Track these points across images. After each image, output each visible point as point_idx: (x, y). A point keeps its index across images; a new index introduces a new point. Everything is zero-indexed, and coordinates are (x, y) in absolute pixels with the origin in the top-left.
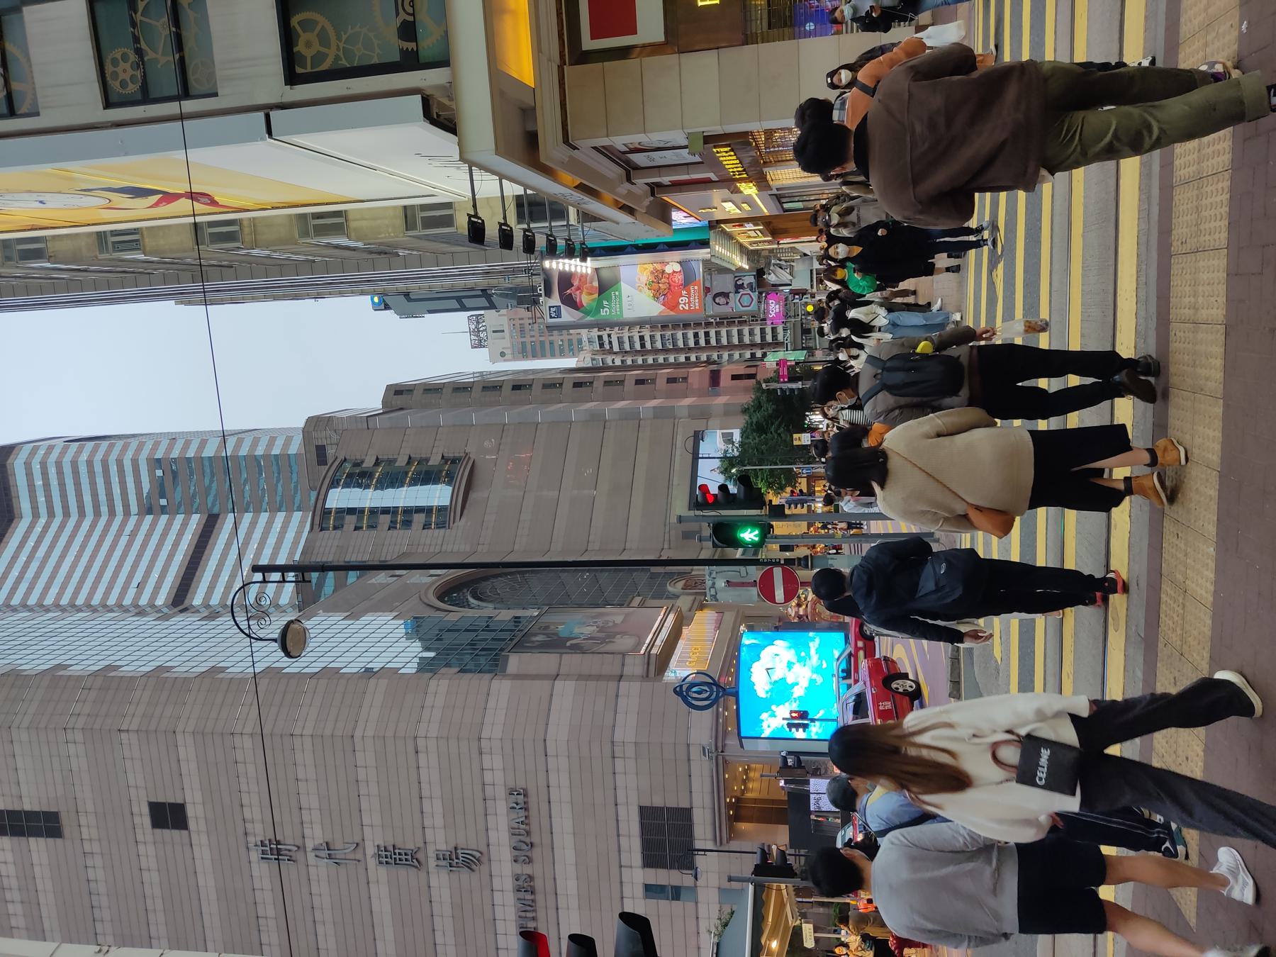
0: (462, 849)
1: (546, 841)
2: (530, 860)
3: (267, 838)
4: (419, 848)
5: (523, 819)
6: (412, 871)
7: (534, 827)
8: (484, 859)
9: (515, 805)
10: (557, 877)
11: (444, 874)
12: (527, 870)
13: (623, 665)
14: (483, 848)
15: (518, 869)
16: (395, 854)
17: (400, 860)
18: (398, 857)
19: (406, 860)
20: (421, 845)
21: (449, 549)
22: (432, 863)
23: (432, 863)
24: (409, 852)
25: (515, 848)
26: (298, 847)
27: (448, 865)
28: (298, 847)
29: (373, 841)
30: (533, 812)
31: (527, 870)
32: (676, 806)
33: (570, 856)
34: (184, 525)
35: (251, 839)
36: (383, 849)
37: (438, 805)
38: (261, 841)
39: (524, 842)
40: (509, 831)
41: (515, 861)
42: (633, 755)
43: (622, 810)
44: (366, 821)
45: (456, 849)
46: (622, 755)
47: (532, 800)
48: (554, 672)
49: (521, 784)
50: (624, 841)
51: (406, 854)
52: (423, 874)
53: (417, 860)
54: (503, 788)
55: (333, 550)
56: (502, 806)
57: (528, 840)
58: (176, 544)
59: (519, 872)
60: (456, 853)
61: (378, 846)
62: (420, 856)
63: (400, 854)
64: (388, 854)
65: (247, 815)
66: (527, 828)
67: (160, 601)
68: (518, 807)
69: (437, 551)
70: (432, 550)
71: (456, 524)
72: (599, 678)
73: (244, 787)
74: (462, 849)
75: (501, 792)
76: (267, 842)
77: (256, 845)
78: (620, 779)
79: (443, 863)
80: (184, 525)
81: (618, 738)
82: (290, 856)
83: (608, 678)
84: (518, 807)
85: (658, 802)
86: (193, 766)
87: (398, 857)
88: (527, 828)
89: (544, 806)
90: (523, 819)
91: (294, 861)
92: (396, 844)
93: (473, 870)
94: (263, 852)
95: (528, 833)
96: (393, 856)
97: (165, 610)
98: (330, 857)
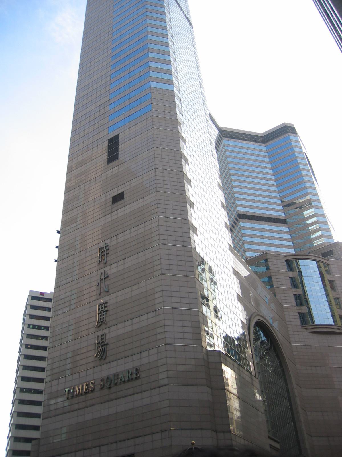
0: (107, 348)
2: (102, 388)
3: (110, 248)
4: (107, 324)
5: (123, 380)
9: (130, 373)
14: (107, 360)
16: (103, 312)
17: (101, 316)
18: (102, 314)
19: (101, 319)
22: (100, 333)
24: (104, 319)
25: (108, 378)
26: (106, 263)
27: (99, 342)
28: (106, 263)
29: (110, 300)
34: (278, 210)
35: (109, 241)
36: (106, 305)
37: (129, 329)
38: (108, 246)
40: (116, 373)
41: (101, 380)
44: (119, 293)
45: (107, 344)
49: (142, 375)
51: (103, 318)
53: (101, 325)
55: (275, 269)
56: (129, 366)
57: (112, 385)
58: (267, 209)
59: (97, 383)
61: (107, 303)
62: (103, 326)
63: (103, 315)
64: (104, 309)
65: (119, 236)
66: (118, 383)
67: (239, 209)
68: (129, 376)
69: (287, 323)
70: (287, 320)
71: (305, 330)
73: (132, 230)
75: (136, 364)
76: (107, 248)
77: (106, 244)
79: (100, 338)
80: (278, 210)
82: (101, 261)
86: (142, 204)
87: (102, 314)
90: (123, 380)
91: (99, 263)
92: (108, 312)
94: (103, 248)
95: (116, 384)
96: (102, 312)
97: (235, 212)
98: (101, 280)
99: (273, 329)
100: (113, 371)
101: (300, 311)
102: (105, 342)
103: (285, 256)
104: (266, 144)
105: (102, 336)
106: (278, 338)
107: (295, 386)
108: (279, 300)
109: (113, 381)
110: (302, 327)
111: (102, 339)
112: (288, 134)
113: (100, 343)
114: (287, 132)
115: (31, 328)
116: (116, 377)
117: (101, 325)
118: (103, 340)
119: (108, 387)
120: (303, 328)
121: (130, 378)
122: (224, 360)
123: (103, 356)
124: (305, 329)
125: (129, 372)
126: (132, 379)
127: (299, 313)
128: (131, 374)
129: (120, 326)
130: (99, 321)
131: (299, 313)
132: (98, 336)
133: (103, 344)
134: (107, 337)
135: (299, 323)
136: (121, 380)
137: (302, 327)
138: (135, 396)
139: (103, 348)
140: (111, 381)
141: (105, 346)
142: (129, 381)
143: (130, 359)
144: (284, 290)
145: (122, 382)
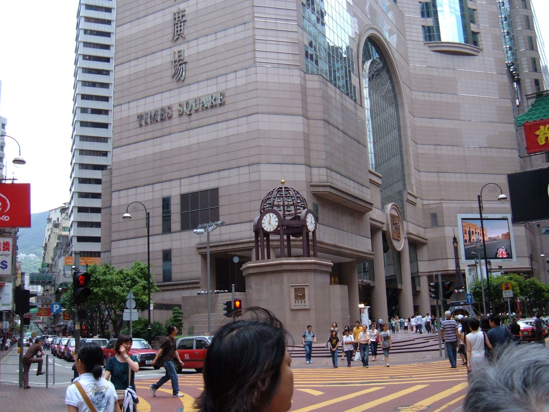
0: (185, 67)
1: (195, 124)
2: (181, 115)
4: (185, 38)
6: (171, 37)
7: (201, 114)
8: (180, 83)
9: (214, 98)
10: (172, 135)
11: (170, 58)
12: (175, 114)
13: (319, 167)
14: (186, 82)
15: (176, 108)
20: (187, 38)
21: (409, 46)
22: (176, 49)
23: (176, 49)
25: (187, 103)
30: (210, 112)
31: (175, 114)
32: (220, 214)
33: (184, 143)
37: (211, 45)
39: (191, 109)
41: (180, 105)
42: (252, 180)
43: (215, 175)
45: (185, 63)
46: (251, 171)
47: (219, 110)
48: (310, 114)
49: (228, 100)
50: (196, 179)
52: (169, 44)
53: (178, 38)
54: (224, 88)
57: (193, 112)
59: (174, 109)
60: (182, 64)
62: (180, 40)
68: (213, 101)
69: (407, 38)
71: (428, 48)
72: (307, 149)
74: (185, 67)
75: (221, 88)
78: (234, 172)
81: (263, 167)
83: (307, 156)
84: (213, 101)
85: (222, 201)
88: (200, 110)
89: (214, 119)
90: (206, 106)
93: (173, 77)
95: (197, 111)
99: (388, 45)
102: (183, 60)
105: (179, 52)
106: (394, 57)
107: (407, 114)
109: (194, 107)
111: (179, 56)
113: (178, 61)
115: (89, 110)
116: (198, 103)
117: (178, 38)
118: (182, 58)
119: (189, 113)
120: (426, 45)
121: (214, 104)
122: (325, 85)
123: (181, 76)
125: (212, 97)
126: (216, 105)
128: (215, 100)
129: (201, 40)
130: (176, 35)
132: (175, 53)
133: (181, 62)
134: (186, 54)
136: (203, 106)
137: (425, 44)
138: (220, 124)
139: (181, 67)
140: (192, 106)
141: (184, 65)
142: (212, 107)
143: (214, 81)
145: (204, 108)
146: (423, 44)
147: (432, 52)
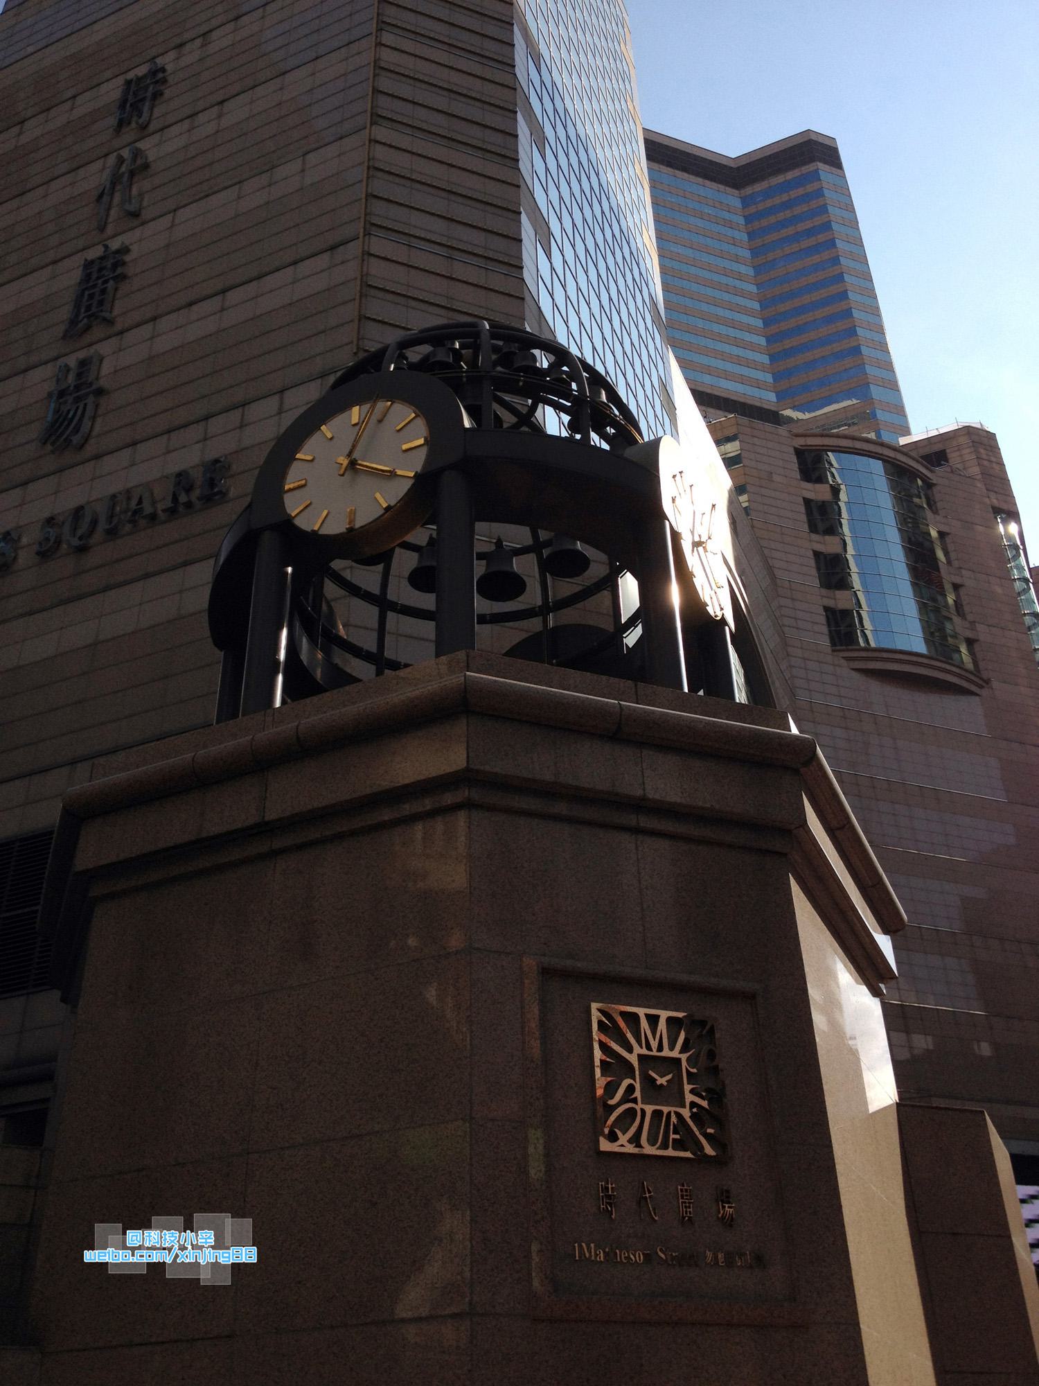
62: (98, 331)
69: (786, 629)
100: (115, 486)
101: (831, 603)
103: (797, 436)
104: (742, 191)
108: (766, 551)
110: (833, 651)
112: (814, 164)
114: (812, 160)
117: (88, 328)
120: (835, 653)
124: (843, 658)
126: (189, 505)
127: (826, 609)
131: (826, 609)
135: (825, 642)
142: (172, 512)
144: (782, 534)
146: (830, 652)
147: (853, 672)
